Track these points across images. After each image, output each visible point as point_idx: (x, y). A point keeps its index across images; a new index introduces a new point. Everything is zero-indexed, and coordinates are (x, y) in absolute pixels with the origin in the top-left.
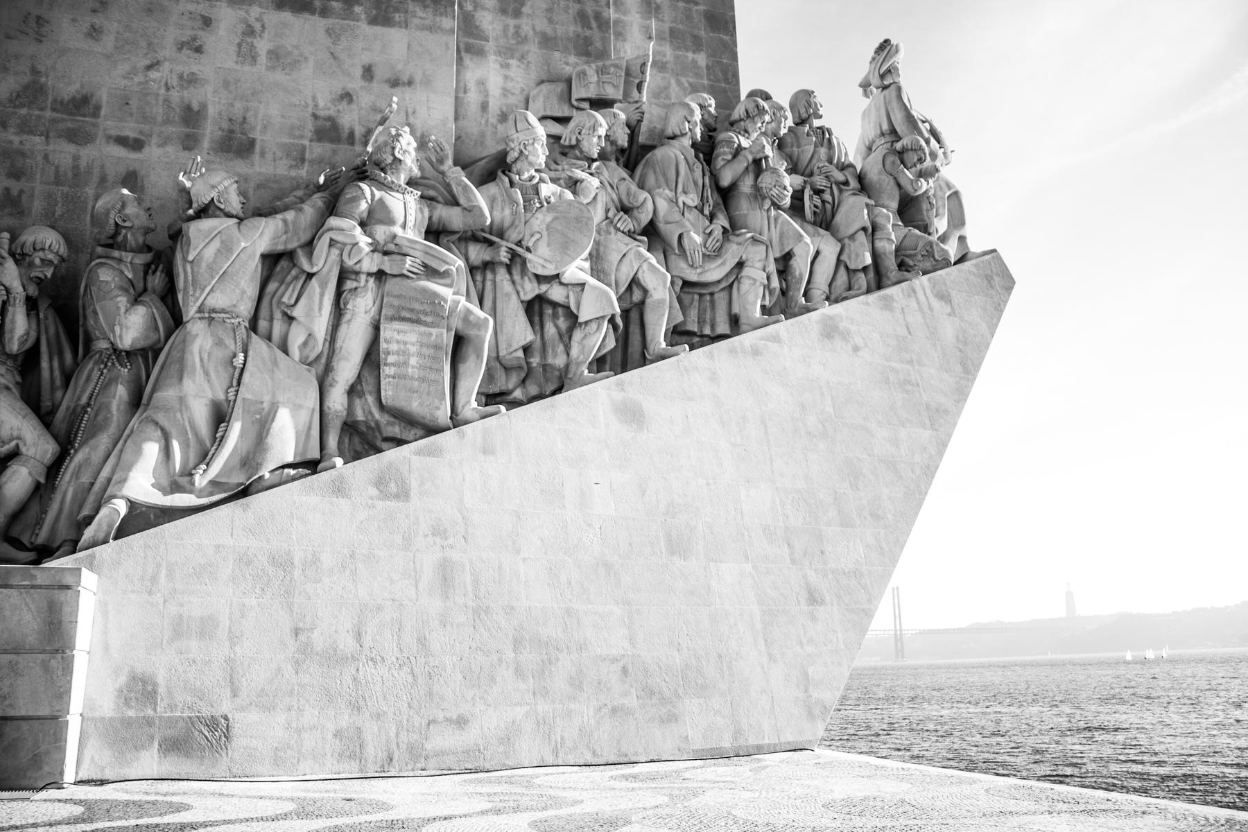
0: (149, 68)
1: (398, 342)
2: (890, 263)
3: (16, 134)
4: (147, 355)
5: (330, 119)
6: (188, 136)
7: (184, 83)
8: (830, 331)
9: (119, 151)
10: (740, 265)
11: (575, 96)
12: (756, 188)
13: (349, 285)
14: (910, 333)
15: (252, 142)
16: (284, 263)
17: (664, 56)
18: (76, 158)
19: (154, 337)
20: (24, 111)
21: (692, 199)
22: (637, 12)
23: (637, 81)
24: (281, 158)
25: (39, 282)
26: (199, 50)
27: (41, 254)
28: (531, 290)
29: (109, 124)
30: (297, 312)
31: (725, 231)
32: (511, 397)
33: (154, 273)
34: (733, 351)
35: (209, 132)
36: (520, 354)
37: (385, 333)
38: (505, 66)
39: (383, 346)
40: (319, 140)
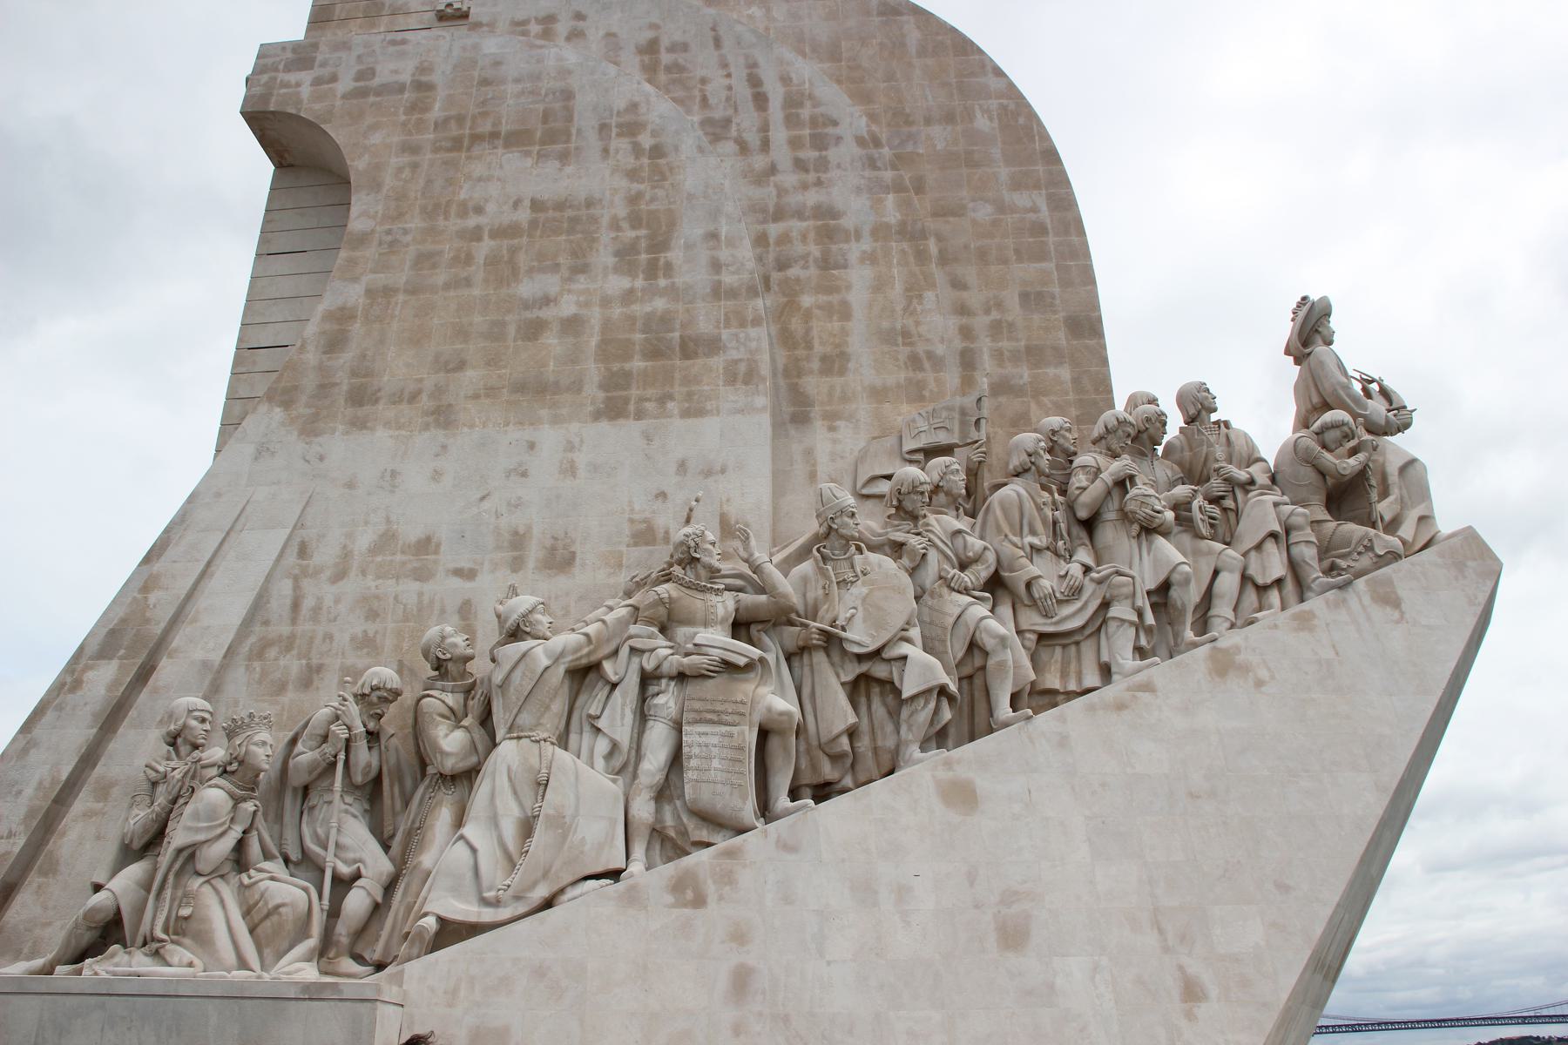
0: (483, 498)
1: (700, 745)
3: (374, 581)
4: (466, 777)
5: (645, 521)
6: (515, 558)
7: (513, 509)
8: (1223, 666)
9: (456, 582)
13: (652, 689)
14: (1337, 654)
16: (592, 676)
17: (1021, 377)
18: (420, 594)
19: (474, 759)
20: (379, 559)
22: (987, 336)
23: (974, 419)
24: (599, 569)
26: (524, 474)
27: (378, 693)
29: (449, 557)
32: (839, 787)
33: (473, 699)
34: (1091, 708)
35: (534, 554)
38: (832, 429)
39: (685, 750)
40: (636, 544)
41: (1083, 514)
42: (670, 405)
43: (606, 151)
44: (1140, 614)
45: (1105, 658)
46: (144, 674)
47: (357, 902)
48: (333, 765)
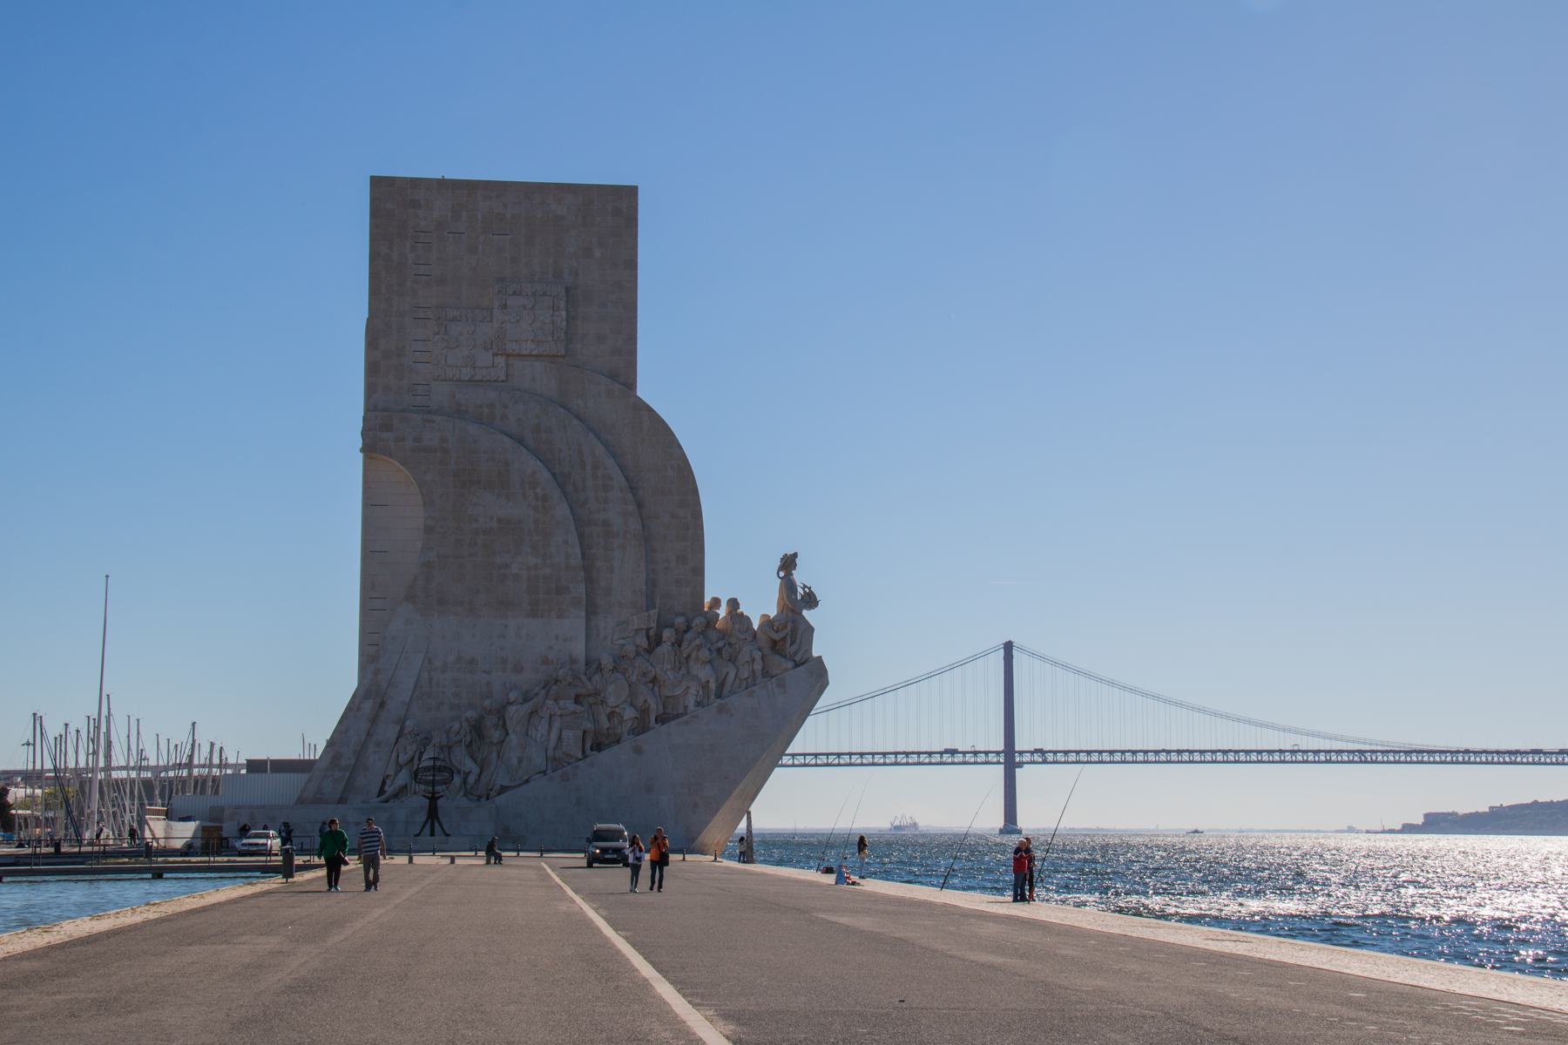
2: (759, 674)
8: (721, 709)
10: (688, 688)
13: (553, 719)
21: (669, 667)
25: (472, 725)
26: (504, 637)
28: (609, 710)
37: (563, 733)
41: (685, 656)
44: (698, 692)
46: (382, 705)
47: (472, 779)
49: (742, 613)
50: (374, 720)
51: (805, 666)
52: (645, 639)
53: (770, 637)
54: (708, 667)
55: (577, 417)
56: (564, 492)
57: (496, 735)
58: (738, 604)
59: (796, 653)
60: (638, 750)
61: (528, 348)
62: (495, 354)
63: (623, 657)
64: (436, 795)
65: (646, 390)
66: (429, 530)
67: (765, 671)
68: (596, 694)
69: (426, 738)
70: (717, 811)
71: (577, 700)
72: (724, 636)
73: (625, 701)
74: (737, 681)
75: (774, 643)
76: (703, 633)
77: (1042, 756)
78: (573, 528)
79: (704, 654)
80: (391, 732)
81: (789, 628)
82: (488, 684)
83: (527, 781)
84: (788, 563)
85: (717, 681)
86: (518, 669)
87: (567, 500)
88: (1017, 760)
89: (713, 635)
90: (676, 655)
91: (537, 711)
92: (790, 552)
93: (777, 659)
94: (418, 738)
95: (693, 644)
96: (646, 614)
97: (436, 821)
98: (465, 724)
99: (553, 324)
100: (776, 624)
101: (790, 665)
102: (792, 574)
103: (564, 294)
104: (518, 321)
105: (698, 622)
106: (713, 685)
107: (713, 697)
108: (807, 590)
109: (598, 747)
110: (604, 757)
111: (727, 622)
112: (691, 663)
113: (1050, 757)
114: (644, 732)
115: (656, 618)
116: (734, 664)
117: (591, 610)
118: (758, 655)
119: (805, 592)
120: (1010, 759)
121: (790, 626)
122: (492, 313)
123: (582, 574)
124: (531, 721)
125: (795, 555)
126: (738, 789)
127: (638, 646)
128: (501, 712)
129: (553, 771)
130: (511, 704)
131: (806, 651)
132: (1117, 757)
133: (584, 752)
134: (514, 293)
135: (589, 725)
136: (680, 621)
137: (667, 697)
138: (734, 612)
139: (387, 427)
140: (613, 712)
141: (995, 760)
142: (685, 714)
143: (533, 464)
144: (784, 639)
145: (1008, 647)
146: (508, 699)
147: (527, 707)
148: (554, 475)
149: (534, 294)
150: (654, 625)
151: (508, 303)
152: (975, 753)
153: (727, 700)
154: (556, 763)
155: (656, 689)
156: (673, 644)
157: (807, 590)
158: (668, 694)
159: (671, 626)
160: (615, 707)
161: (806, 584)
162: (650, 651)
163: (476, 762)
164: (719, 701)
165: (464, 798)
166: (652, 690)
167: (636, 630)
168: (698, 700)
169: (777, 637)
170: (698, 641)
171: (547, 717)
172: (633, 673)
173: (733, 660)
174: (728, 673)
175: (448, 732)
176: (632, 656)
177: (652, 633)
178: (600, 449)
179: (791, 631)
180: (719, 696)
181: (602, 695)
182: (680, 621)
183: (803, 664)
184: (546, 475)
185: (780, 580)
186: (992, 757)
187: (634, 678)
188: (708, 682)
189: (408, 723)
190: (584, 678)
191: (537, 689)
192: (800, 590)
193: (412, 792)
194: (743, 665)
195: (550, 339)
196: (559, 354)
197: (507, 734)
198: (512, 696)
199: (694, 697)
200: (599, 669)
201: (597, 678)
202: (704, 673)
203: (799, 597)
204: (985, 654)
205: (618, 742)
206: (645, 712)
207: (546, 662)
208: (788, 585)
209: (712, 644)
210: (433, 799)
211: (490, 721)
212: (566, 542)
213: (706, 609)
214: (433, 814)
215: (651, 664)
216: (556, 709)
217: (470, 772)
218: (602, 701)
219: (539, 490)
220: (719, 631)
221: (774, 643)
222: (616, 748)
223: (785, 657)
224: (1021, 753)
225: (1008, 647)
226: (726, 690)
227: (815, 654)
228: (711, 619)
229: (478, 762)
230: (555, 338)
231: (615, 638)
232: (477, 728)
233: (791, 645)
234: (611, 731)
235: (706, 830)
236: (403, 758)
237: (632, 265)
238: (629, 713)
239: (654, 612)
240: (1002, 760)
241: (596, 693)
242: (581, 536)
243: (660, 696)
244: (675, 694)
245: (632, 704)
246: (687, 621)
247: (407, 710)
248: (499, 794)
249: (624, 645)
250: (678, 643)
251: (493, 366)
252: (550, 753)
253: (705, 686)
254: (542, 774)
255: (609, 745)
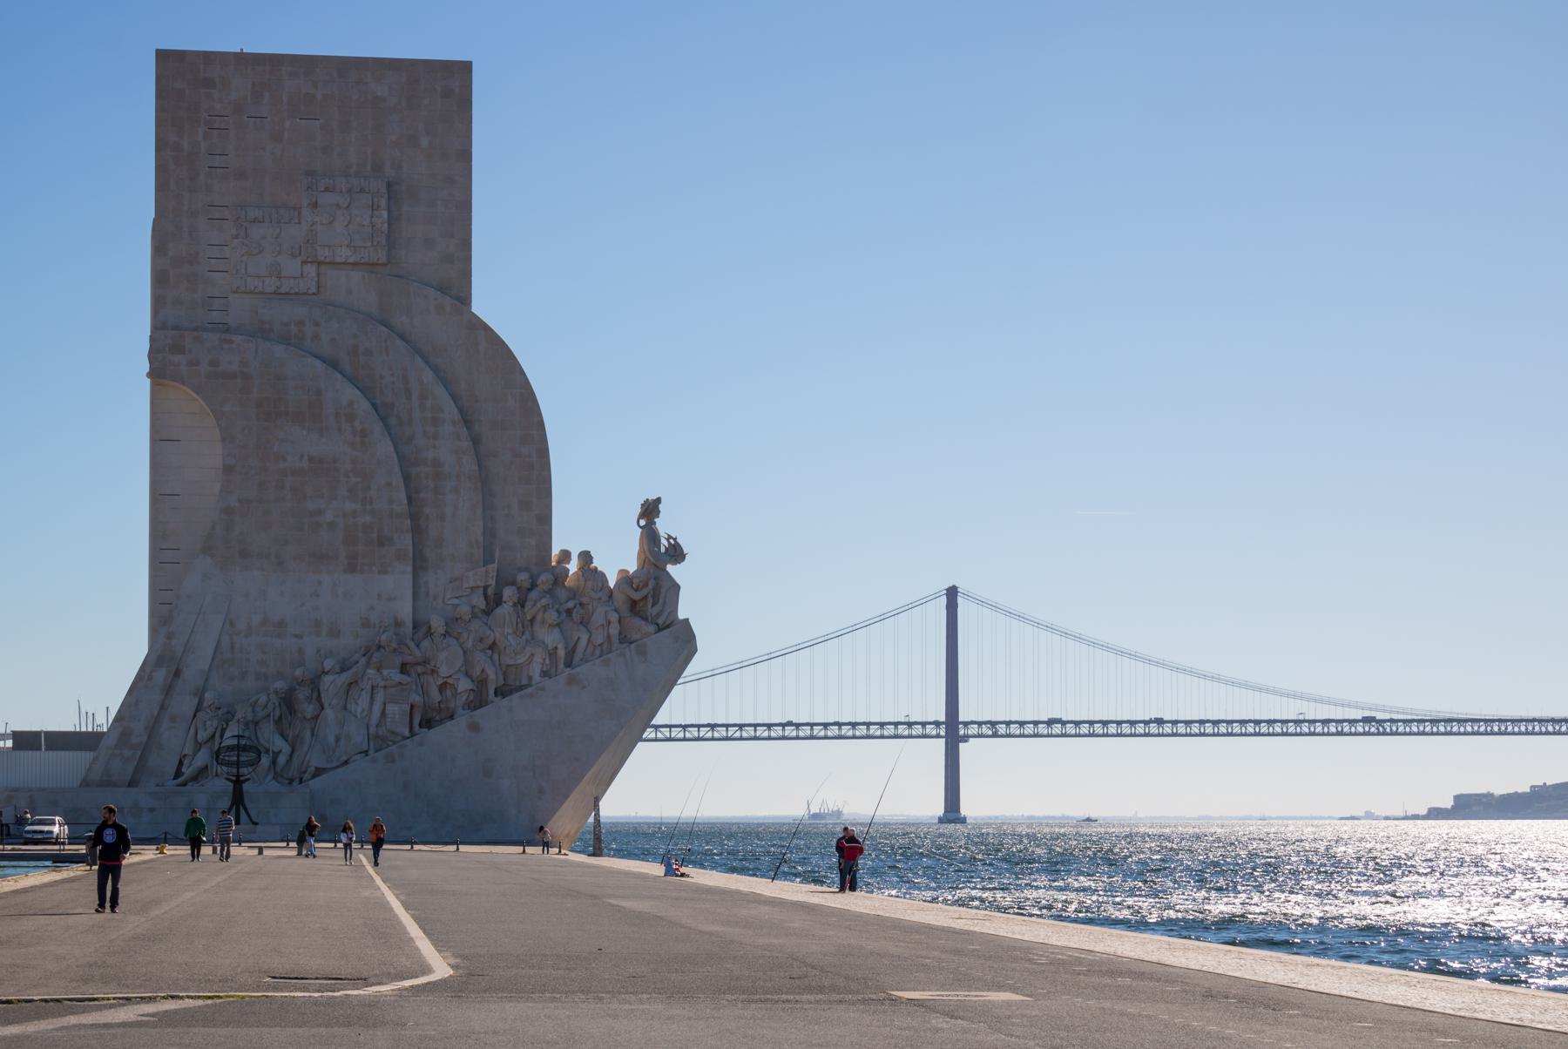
2: (615, 639)
8: (571, 681)
10: (533, 655)
11: (464, 587)
12: (543, 618)
13: (375, 691)
15: (339, 631)
21: (510, 631)
26: (318, 596)
28: (440, 681)
30: (359, 702)
31: (527, 641)
36: (437, 705)
41: (529, 618)
42: (374, 568)
43: (340, 429)
44: (544, 659)
45: (531, 674)
46: (177, 673)
47: (282, 759)
48: (269, 715)
49: (596, 568)
50: (168, 690)
51: (671, 629)
52: (482, 599)
53: (631, 599)
54: (556, 631)
55: (402, 337)
56: (387, 427)
57: (309, 710)
58: (591, 558)
59: (658, 615)
60: (475, 727)
61: (343, 254)
62: (304, 262)
63: (457, 619)
64: (242, 778)
65: (482, 306)
66: (228, 470)
67: (623, 636)
68: (425, 662)
69: (228, 712)
70: (566, 797)
71: (404, 669)
72: (575, 595)
73: (459, 670)
74: (590, 646)
75: (633, 604)
76: (549, 591)
77: (994, 729)
78: (397, 469)
79: (552, 616)
80: (184, 704)
81: (650, 587)
82: (300, 651)
83: (346, 763)
84: (650, 510)
85: (566, 648)
86: (335, 633)
87: (390, 434)
88: (962, 732)
89: (562, 594)
90: (518, 617)
91: (356, 682)
92: (652, 497)
93: (637, 622)
94: (220, 712)
95: (539, 605)
96: (484, 569)
97: (241, 808)
98: (273, 697)
99: (373, 226)
100: (636, 581)
101: (652, 628)
102: (655, 523)
103: (385, 191)
104: (330, 223)
105: (544, 579)
106: (561, 652)
107: (561, 665)
108: (672, 541)
109: (428, 723)
110: (436, 734)
111: (578, 581)
112: (537, 627)
113: (1002, 729)
114: (481, 706)
115: (495, 574)
116: (586, 627)
117: (419, 565)
118: (614, 617)
119: (669, 543)
120: (953, 731)
121: (651, 583)
122: (299, 213)
123: (409, 521)
124: (350, 693)
125: (658, 500)
126: (590, 773)
127: (473, 607)
128: (314, 683)
129: (377, 751)
130: (327, 673)
131: (670, 613)
132: (1085, 729)
133: (411, 729)
134: (327, 190)
135: (417, 699)
136: (522, 578)
137: (508, 666)
138: (586, 568)
139: (178, 348)
140: (446, 683)
141: (934, 733)
142: (529, 685)
143: (349, 393)
144: (645, 598)
145: (952, 593)
146: (323, 668)
147: (345, 677)
148: (374, 406)
149: (349, 191)
150: (492, 582)
151: (320, 201)
152: (910, 725)
153: (578, 669)
154: (380, 741)
155: (496, 656)
156: (515, 605)
157: (672, 541)
158: (511, 662)
159: (513, 583)
160: (447, 677)
161: (672, 535)
162: (488, 612)
163: (286, 741)
164: (568, 671)
165: (274, 781)
166: (491, 658)
167: (472, 588)
168: (544, 669)
169: (637, 596)
170: (544, 601)
171: (369, 687)
172: (468, 638)
173: (584, 623)
174: (579, 638)
175: (253, 706)
176: (467, 618)
177: (490, 591)
178: (428, 376)
179: (654, 589)
180: (569, 664)
181: (433, 664)
182: (522, 578)
183: (668, 627)
184: (363, 405)
185: (640, 530)
186: (930, 730)
187: (469, 644)
188: (556, 648)
189: (207, 695)
190: (411, 644)
191: (356, 657)
192: (664, 542)
193: (214, 774)
194: (597, 629)
195: (369, 244)
196: (380, 262)
197: (323, 708)
198: (328, 665)
199: (540, 666)
200: (429, 633)
201: (426, 644)
202: (552, 638)
203: (663, 550)
204: (923, 602)
205: (452, 717)
206: (482, 682)
207: (366, 624)
208: (650, 536)
209: (561, 604)
210: (238, 782)
211: (302, 694)
212: (389, 484)
213: (553, 564)
214: (238, 800)
215: (490, 627)
216: (379, 680)
217: (280, 752)
218: (433, 671)
219: (357, 424)
220: (568, 589)
221: (633, 604)
222: (449, 724)
223: (646, 619)
224: (966, 724)
225: (952, 593)
226: (577, 659)
227: (681, 615)
228: (559, 576)
229: (290, 738)
230: (375, 243)
231: (448, 596)
232: (288, 701)
233: (653, 606)
234: (442, 706)
235: (554, 819)
236: (202, 736)
237: (466, 156)
238: (464, 685)
239: (493, 567)
240: (943, 733)
241: (425, 662)
242: (407, 478)
243: (500, 665)
244: (519, 661)
245: (467, 674)
246: (531, 577)
247: (207, 680)
248: (314, 776)
249: (457, 605)
250: (521, 603)
251: (302, 276)
252: (372, 730)
253: (553, 654)
254: (364, 755)
255: (441, 722)
